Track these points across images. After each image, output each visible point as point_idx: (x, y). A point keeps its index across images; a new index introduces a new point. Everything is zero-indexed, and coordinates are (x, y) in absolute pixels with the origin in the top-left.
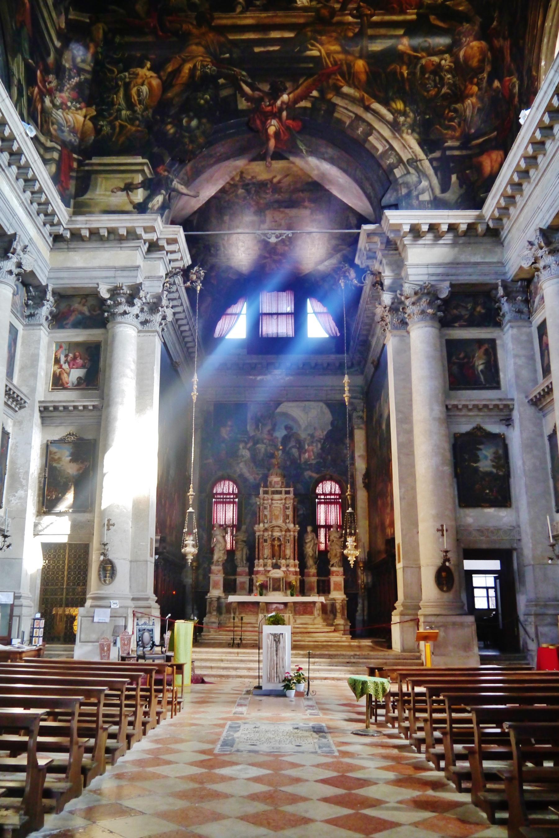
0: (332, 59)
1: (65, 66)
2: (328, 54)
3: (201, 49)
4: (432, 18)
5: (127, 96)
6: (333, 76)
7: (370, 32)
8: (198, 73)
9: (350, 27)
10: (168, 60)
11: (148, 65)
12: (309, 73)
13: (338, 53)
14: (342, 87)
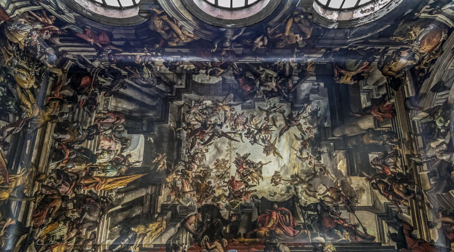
0: (13, 180)
1: (48, 48)
2: (16, 178)
3: (36, 114)
4: (25, 236)
5: (24, 68)
6: (3, 179)
7: (24, 202)
8: (24, 108)
10: (35, 97)
11: (35, 87)
12: (9, 165)
13: (16, 184)
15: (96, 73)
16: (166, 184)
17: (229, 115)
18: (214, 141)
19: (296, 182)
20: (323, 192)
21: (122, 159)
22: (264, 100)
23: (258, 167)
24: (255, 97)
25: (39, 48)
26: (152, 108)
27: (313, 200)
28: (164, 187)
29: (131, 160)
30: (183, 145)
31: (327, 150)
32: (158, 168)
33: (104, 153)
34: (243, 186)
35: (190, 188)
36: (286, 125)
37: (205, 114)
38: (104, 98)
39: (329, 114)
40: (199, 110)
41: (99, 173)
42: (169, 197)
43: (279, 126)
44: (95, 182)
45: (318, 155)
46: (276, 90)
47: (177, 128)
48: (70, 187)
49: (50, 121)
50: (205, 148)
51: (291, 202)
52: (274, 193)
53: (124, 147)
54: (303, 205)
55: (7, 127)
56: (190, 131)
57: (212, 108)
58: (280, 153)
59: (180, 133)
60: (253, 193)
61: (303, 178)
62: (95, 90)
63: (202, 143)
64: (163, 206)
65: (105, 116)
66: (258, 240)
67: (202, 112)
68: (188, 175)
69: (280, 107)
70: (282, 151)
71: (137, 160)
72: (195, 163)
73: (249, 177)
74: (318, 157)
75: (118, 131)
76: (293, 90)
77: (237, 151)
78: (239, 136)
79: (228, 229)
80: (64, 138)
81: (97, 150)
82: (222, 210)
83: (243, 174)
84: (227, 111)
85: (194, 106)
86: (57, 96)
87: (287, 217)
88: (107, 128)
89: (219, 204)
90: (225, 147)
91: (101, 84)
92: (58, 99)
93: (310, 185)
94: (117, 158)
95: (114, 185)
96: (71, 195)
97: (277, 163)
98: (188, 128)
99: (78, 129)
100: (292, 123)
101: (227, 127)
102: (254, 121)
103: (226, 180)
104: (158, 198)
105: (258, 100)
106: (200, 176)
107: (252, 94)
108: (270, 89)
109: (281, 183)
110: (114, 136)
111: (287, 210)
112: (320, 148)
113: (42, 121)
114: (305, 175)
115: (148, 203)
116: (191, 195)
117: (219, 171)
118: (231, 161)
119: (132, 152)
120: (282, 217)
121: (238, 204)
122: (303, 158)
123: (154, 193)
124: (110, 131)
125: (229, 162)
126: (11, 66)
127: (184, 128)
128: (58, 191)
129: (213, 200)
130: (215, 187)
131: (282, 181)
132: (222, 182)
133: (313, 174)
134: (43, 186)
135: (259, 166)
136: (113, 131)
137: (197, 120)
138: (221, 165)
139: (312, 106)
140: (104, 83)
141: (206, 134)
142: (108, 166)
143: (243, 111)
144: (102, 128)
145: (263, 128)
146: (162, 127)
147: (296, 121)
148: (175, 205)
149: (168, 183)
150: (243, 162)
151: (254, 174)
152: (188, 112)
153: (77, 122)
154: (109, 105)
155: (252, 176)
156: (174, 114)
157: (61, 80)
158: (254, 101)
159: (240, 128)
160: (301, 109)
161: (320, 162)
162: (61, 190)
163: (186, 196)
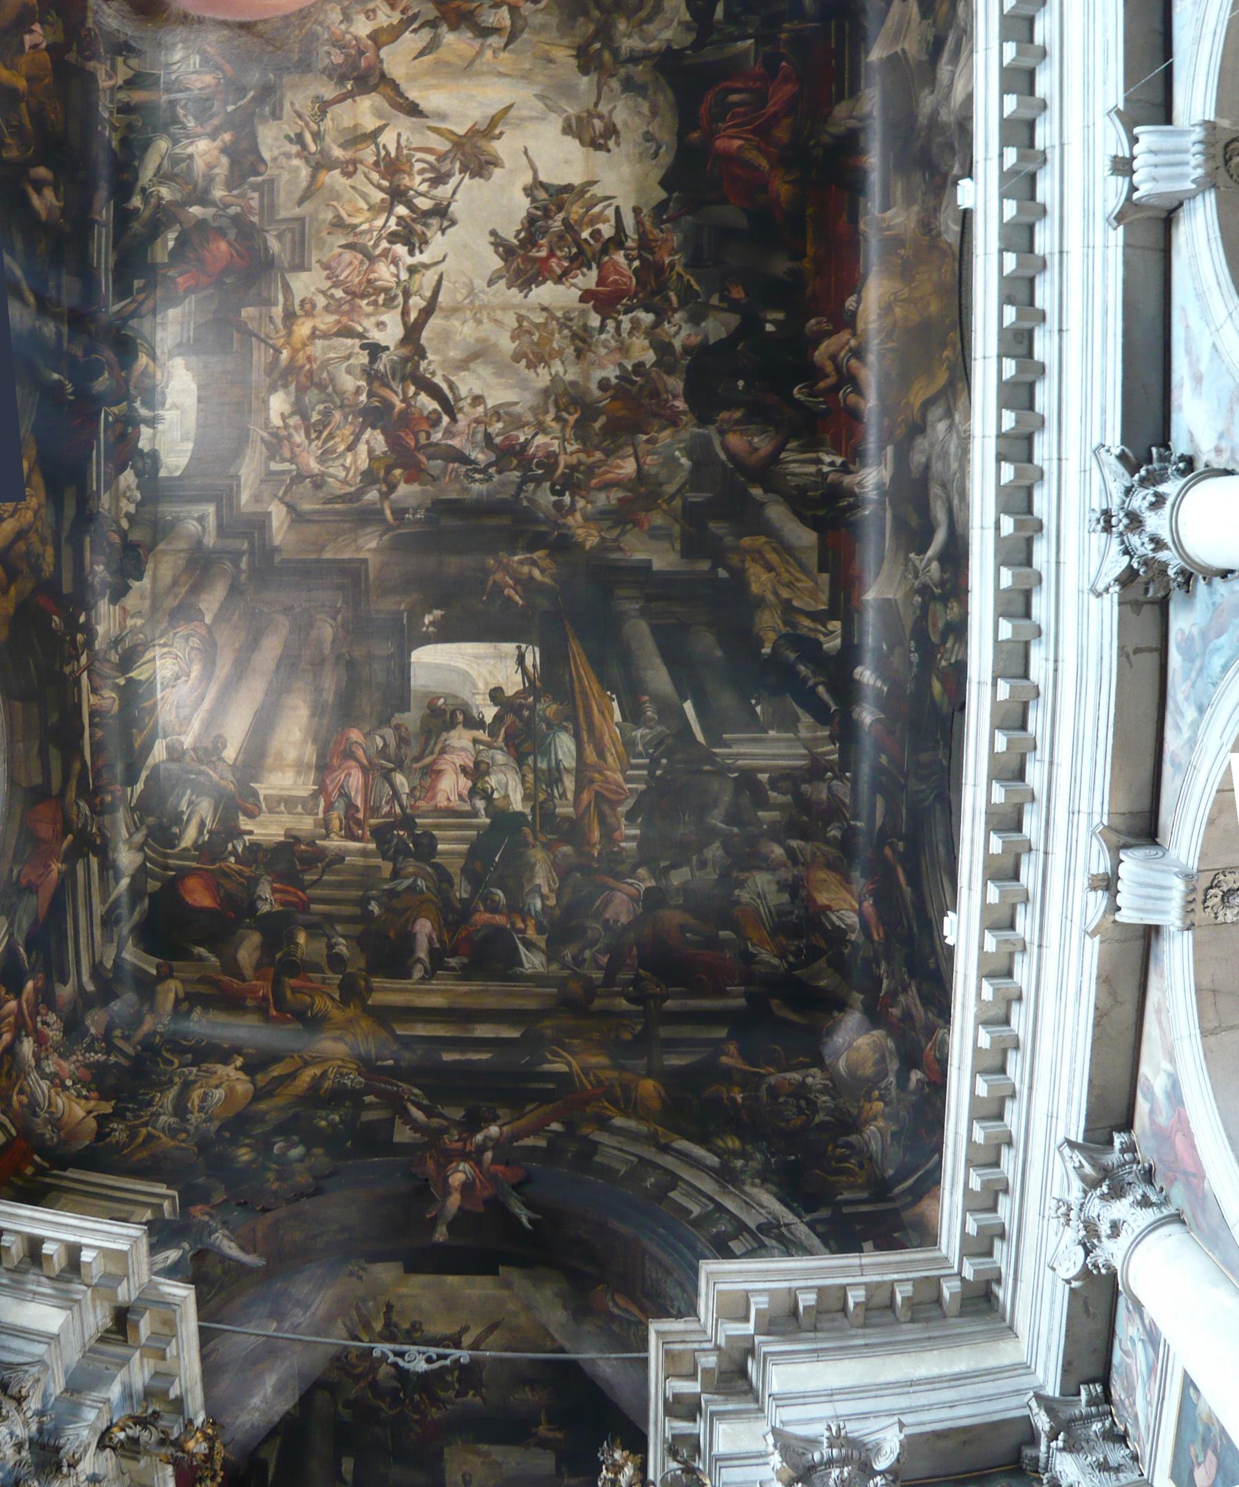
7: (665, 1032)
8: (327, 1084)
9: (625, 1022)
11: (239, 1062)
12: (544, 1097)
13: (604, 1068)
14: (611, 1118)
15: (166, 856)
16: (606, 549)
17: (331, 319)
18: (439, 373)
21: (510, 718)
22: (271, 182)
23: (550, 199)
24: (255, 219)
25: (94, 1057)
29: (513, 683)
30: (454, 496)
33: (484, 790)
34: (620, 257)
35: (623, 458)
37: (327, 414)
38: (262, 817)
40: (311, 441)
41: (563, 795)
42: (655, 534)
43: (380, 117)
44: (597, 807)
46: (227, 137)
47: (385, 520)
48: (613, 889)
49: (363, 1001)
50: (467, 409)
53: (460, 718)
55: (408, 1120)
56: (398, 472)
57: (301, 390)
59: (406, 511)
60: (648, 223)
62: (234, 852)
63: (446, 419)
65: (340, 805)
66: (810, 211)
67: (315, 430)
68: (573, 468)
69: (300, 116)
71: (512, 664)
72: (527, 442)
73: (585, 234)
75: (398, 747)
77: (480, 283)
78: (417, 277)
79: (772, 315)
80: (430, 940)
81: (474, 814)
82: (706, 338)
83: (572, 259)
84: (314, 329)
85: (291, 461)
86: (264, 988)
88: (387, 790)
90: (465, 331)
91: (210, 832)
92: (277, 984)
94: (506, 740)
95: (607, 737)
96: (644, 881)
98: (385, 481)
99: (392, 893)
101: (381, 325)
102: (356, 221)
103: (595, 320)
104: (660, 572)
105: (269, 208)
106: (577, 421)
108: (225, 160)
110: (417, 759)
113: (365, 1024)
116: (649, 453)
118: (520, 306)
119: (481, 686)
121: (687, 277)
124: (399, 779)
125: (523, 312)
126: (186, 1131)
127: (385, 496)
128: (626, 928)
129: (671, 371)
130: (621, 365)
132: (603, 336)
134: (609, 980)
135: (542, 195)
136: (400, 766)
137: (351, 448)
138: (537, 344)
140: (202, 824)
141: (409, 406)
142: (535, 770)
144: (386, 809)
145: (386, 183)
148: (684, 508)
149: (603, 539)
150: (527, 259)
153: (363, 902)
154: (294, 793)
155: (580, 222)
157: (201, 980)
159: (384, 273)
162: (624, 919)
163: (654, 471)
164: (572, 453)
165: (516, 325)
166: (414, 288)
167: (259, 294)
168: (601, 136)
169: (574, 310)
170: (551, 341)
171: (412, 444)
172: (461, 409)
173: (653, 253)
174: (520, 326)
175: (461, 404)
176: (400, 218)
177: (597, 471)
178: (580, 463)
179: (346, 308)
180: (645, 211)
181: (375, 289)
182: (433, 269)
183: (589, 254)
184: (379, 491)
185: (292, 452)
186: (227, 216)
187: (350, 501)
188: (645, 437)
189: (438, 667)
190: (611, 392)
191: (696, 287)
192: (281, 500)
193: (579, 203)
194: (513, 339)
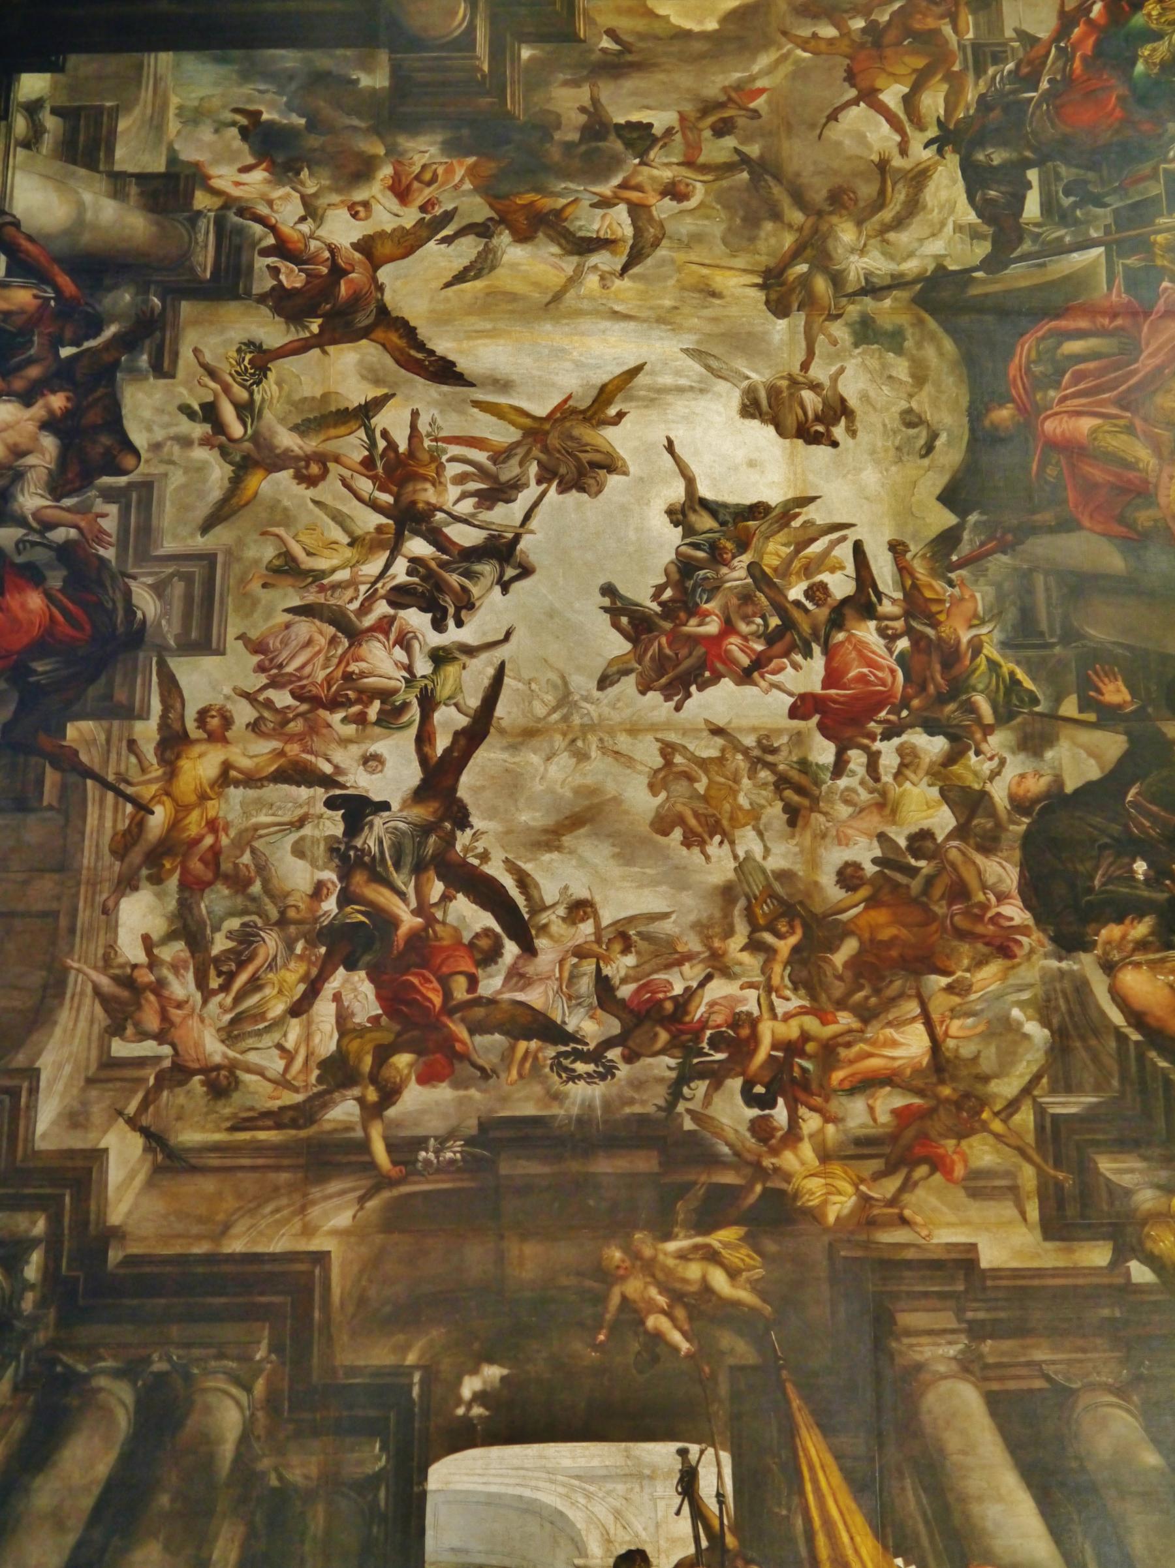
17: (265, 747)
19: (821, 285)
20: (885, 128)
22: (147, 486)
24: (109, 553)
26: (163, 1413)
27: (947, 187)
28: (900, 1236)
30: (529, 1110)
31: (575, 83)
32: (736, 1304)
36: (366, 333)
37: (247, 939)
39: (289, 59)
40: (207, 995)
42: (979, 1186)
43: (377, 382)
45: (606, 144)
46: (58, 401)
47: (372, 1165)
51: (964, 320)
52: (910, 425)
54: (983, 249)
56: (403, 1060)
57: (191, 887)
58: (603, 376)
59: (420, 1143)
60: (920, 569)
61: (788, 240)
63: (511, 950)
64: (1057, 1226)
67: (218, 971)
68: (792, 1048)
69: (212, 373)
70: (579, 365)
71: (668, 1493)
72: (690, 994)
74: (629, 144)
76: (64, 280)
77: (583, 684)
78: (451, 670)
82: (1058, 781)
83: (771, 638)
84: (227, 766)
85: (160, 1037)
87: (1074, 347)
89: (1012, 798)
90: (553, 774)
93: (838, 199)
97: (680, 406)
98: (374, 1079)
100: (356, 300)
101: (371, 761)
102: (322, 564)
103: (823, 752)
104: (996, 1273)
105: (140, 536)
106: (796, 949)
107: (84, 575)
108: (49, 442)
109: (835, 379)
111: (1026, 348)
112: (558, 126)
114: (769, 226)
115: (1039, 1355)
116: (954, 1013)
117: (754, 814)
118: (668, 726)
120: (1079, 377)
121: (1007, 666)
122: (638, 232)
123: (959, 1312)
125: (672, 737)
127: (373, 1112)
129: (989, 845)
130: (882, 837)
131: (819, 372)
132: (843, 782)
133: (755, 178)
135: (705, 522)
137: (298, 1009)
138: (705, 798)
139: (217, 161)
141: (431, 921)
143: (235, 647)
145: (386, 498)
146: (362, 1301)
147: (338, 272)
148: (1040, 1128)
149: (865, 1200)
151: (770, 561)
152: (221, 1083)
155: (784, 571)
156: (230, 1203)
158: (144, 556)
159: (381, 662)
160: (240, 231)
161: (669, 132)
163: (967, 1050)
164: (788, 1017)
165: (659, 762)
166: (443, 692)
167: (109, 697)
168: (818, 419)
169: (779, 732)
170: (734, 793)
171: (437, 1000)
172: (544, 929)
173: (935, 625)
174: (668, 763)
175: (543, 918)
176: (414, 560)
177: (844, 1053)
178: (805, 1037)
179: (296, 726)
180: (913, 548)
181: (361, 691)
182: (484, 656)
183: (806, 628)
184: (361, 1100)
185: (164, 1017)
186: (48, 546)
187: (294, 1124)
188: (944, 981)
189: (493, 1501)
190: (863, 892)
191: (1028, 684)
192: (132, 1123)
193: (781, 537)
194: (653, 788)
